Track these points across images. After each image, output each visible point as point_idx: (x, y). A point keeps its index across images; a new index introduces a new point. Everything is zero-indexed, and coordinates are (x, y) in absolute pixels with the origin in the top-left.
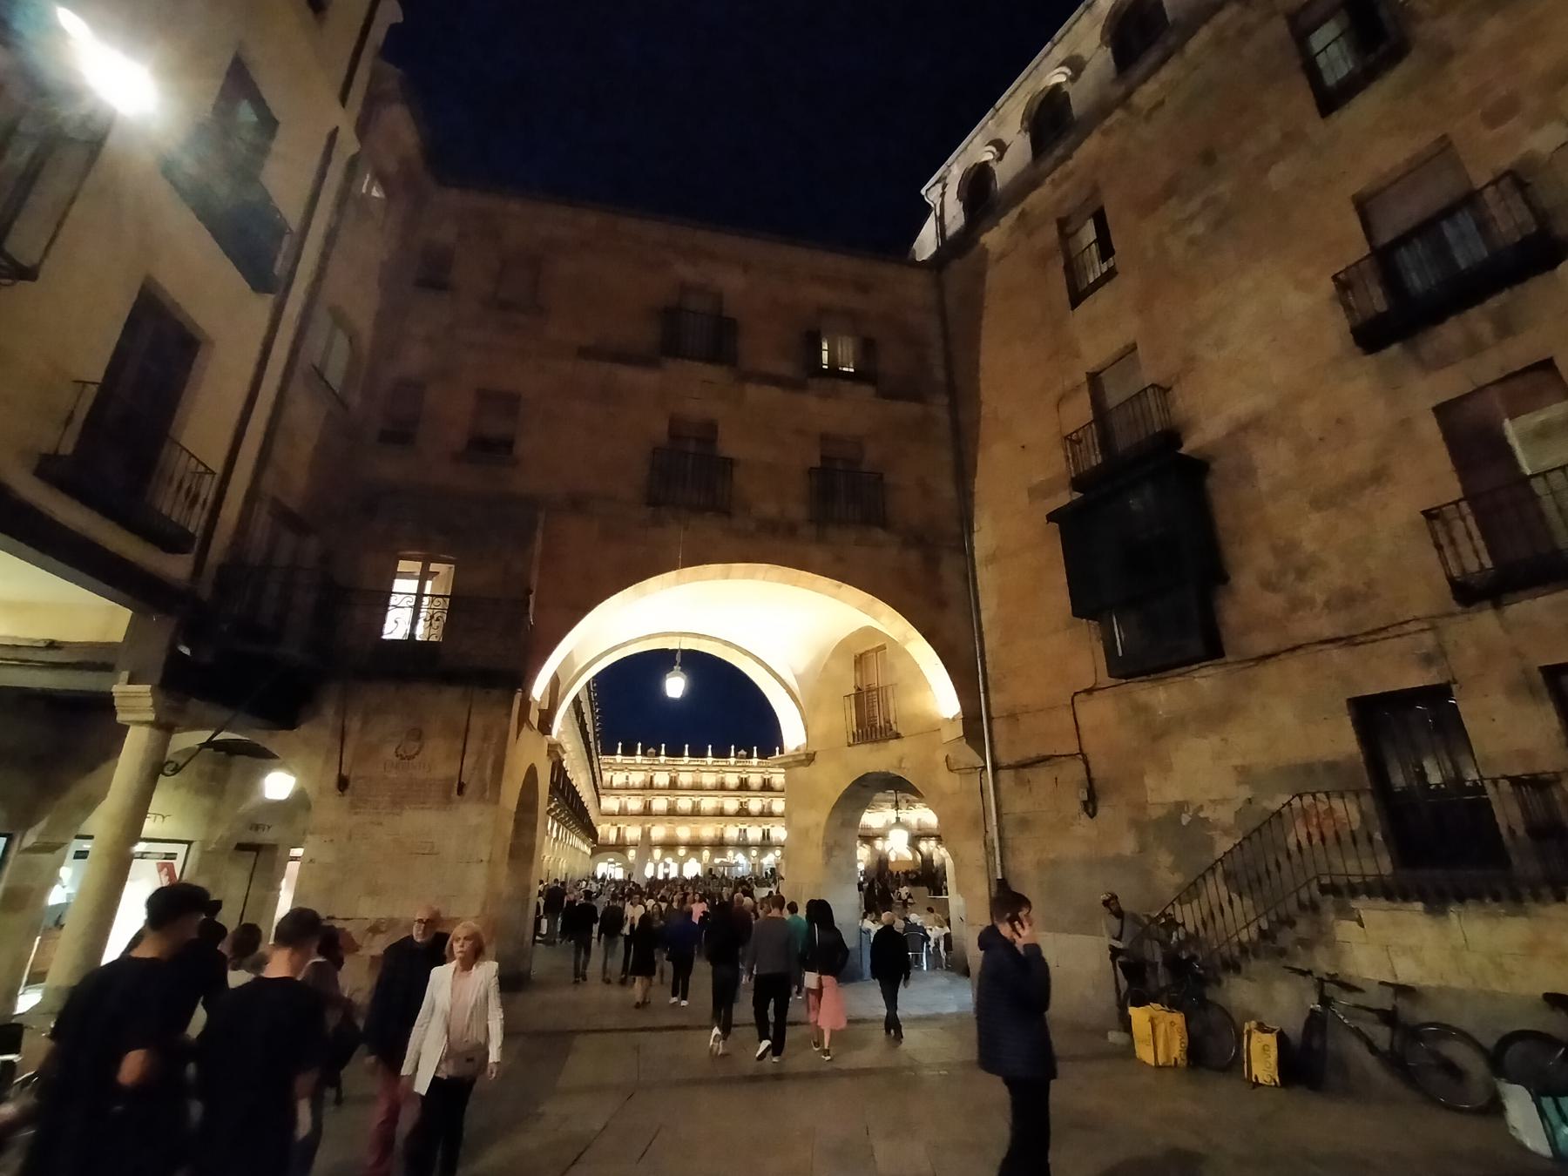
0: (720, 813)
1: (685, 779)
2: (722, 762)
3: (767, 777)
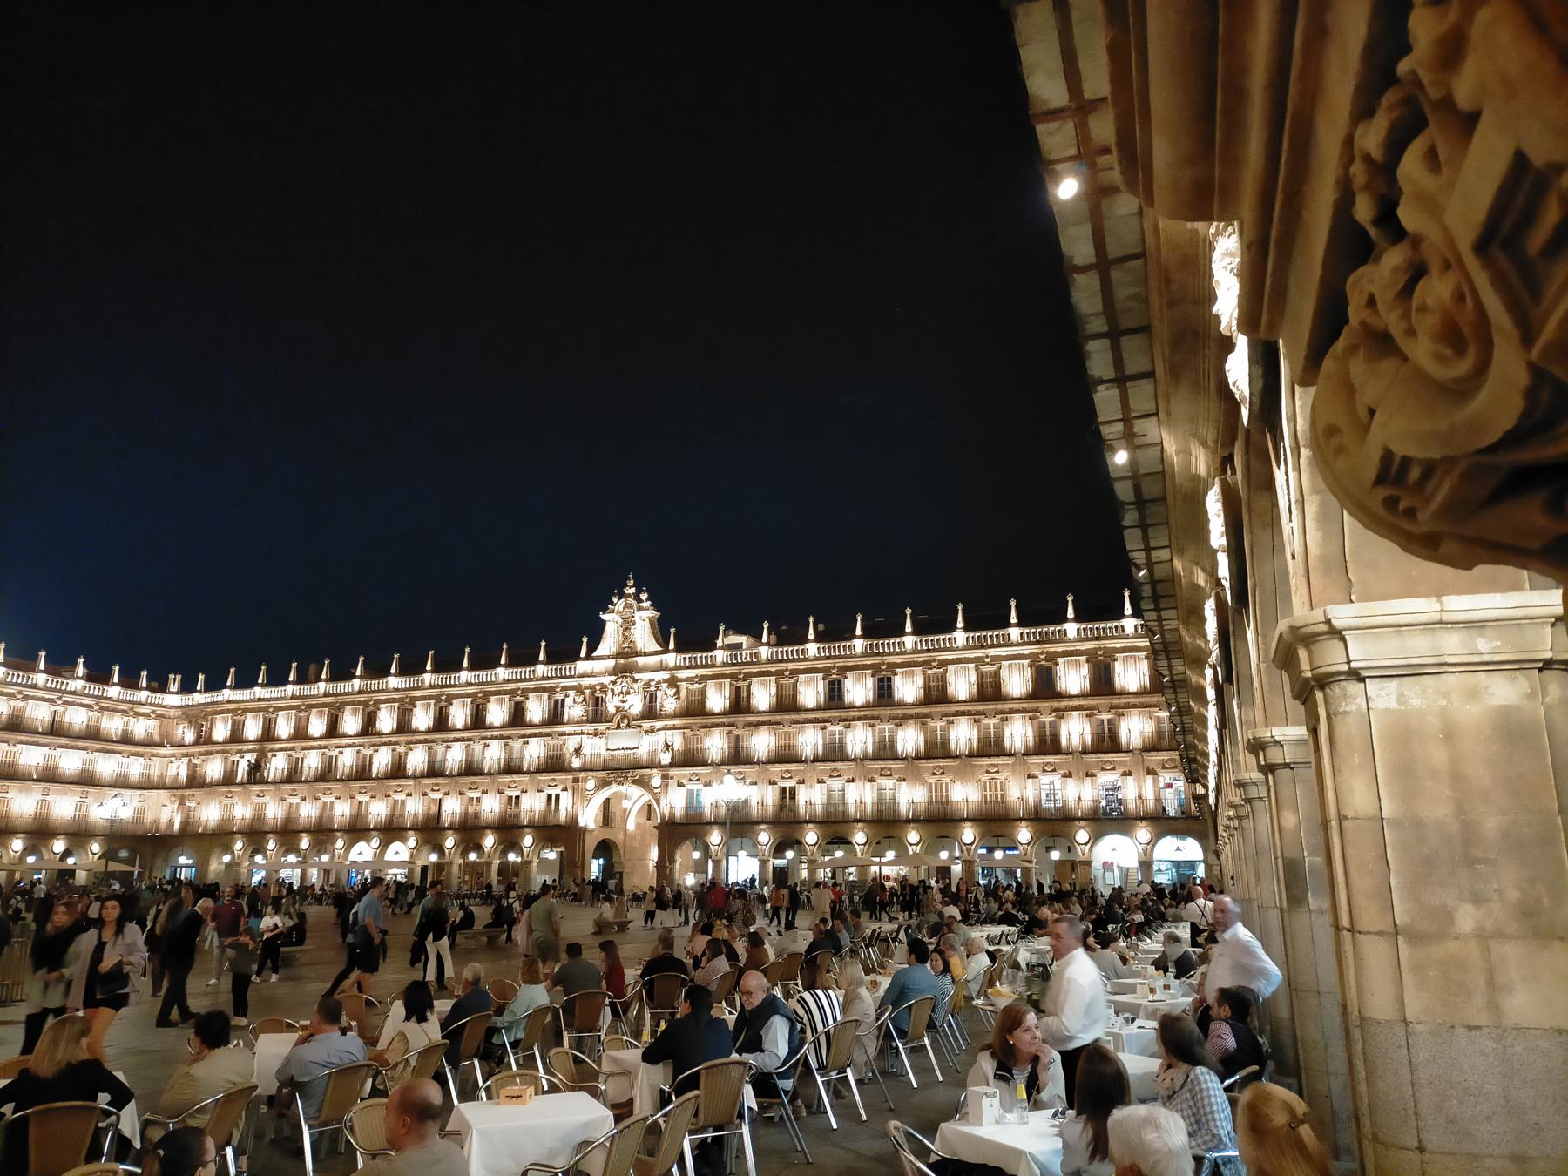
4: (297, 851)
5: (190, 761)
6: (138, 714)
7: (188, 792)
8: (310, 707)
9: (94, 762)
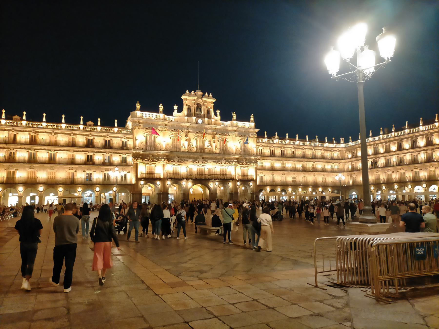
0: (72, 162)
1: (43, 138)
2: (73, 127)
3: (108, 139)
4: (394, 189)
5: (351, 163)
6: (334, 151)
7: (353, 173)
8: (389, 141)
9: (325, 165)
